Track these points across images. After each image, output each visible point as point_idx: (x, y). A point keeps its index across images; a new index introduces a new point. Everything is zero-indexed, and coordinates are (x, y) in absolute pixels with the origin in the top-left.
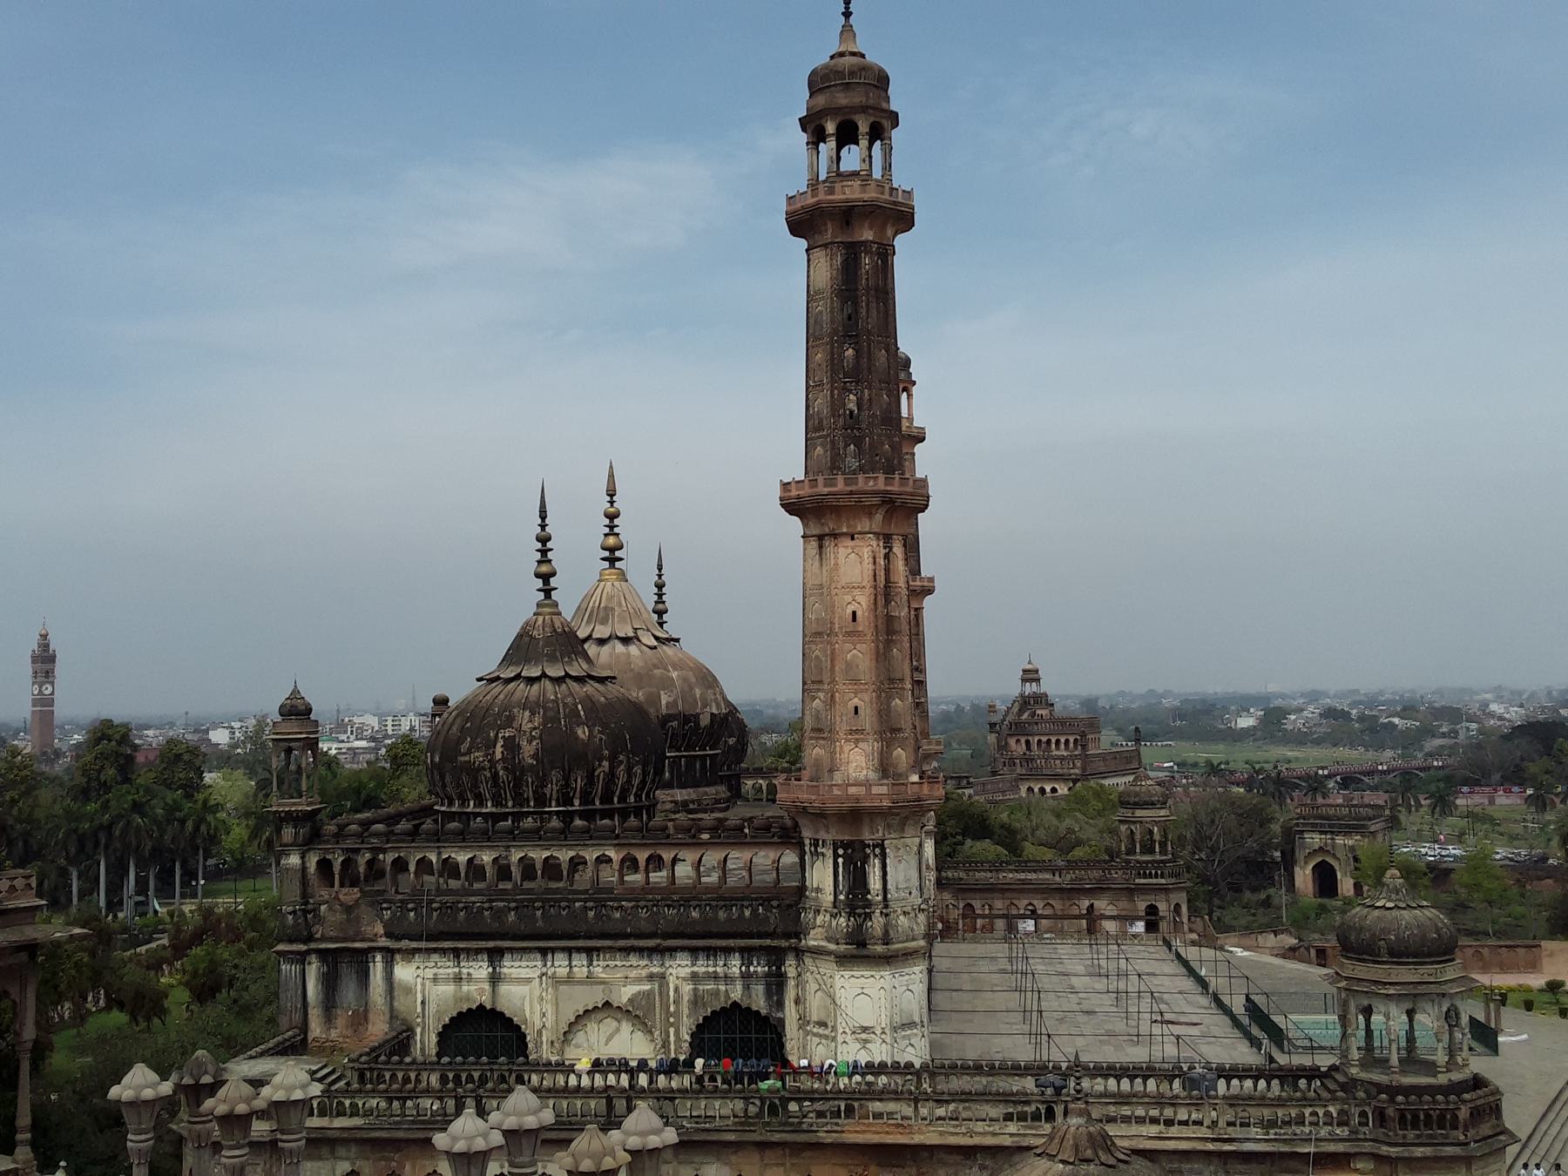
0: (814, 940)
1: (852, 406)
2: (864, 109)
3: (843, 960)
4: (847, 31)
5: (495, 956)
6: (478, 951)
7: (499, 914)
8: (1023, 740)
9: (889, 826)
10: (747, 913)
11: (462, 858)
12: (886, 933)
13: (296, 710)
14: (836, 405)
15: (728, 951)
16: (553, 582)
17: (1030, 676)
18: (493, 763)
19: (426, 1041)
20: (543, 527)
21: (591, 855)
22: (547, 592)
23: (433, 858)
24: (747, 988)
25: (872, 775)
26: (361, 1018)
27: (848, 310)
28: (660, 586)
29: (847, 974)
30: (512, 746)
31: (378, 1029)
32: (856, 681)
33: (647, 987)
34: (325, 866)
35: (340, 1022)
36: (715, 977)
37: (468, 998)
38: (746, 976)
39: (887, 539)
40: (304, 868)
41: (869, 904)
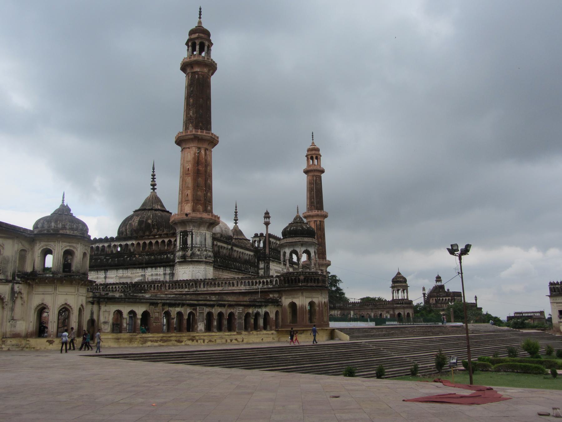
0: (177, 260)
1: (191, 114)
2: (197, 38)
4: (200, 22)
5: (106, 270)
6: (102, 270)
7: (108, 260)
8: (434, 299)
9: (194, 226)
10: (165, 256)
11: (101, 245)
12: (191, 255)
15: (160, 267)
16: (155, 187)
17: (438, 279)
18: (126, 230)
20: (153, 172)
21: (129, 243)
22: (154, 189)
23: (94, 246)
24: (165, 277)
27: (192, 89)
28: (236, 212)
29: (181, 267)
32: (188, 187)
33: (141, 278)
36: (157, 275)
38: (165, 274)
39: (199, 148)
41: (187, 248)
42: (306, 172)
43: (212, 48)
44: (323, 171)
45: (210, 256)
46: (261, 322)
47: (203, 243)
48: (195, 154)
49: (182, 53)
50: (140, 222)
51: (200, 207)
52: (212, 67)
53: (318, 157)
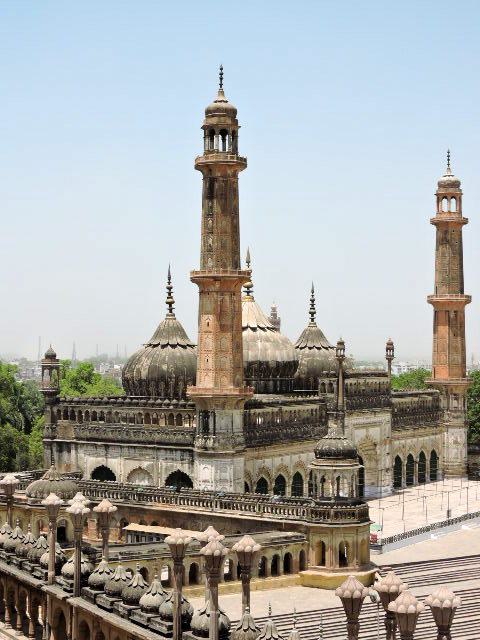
1: (210, 241)
3: (201, 455)
13: (51, 357)
14: (205, 242)
15: (176, 450)
19: (87, 476)
20: (169, 283)
25: (211, 385)
26: (68, 467)
28: (313, 301)
30: (139, 372)
31: (74, 470)
34: (59, 411)
35: (63, 468)
37: (98, 462)
40: (52, 412)
42: (434, 222)
43: (240, 131)
44: (465, 221)
45: (240, 444)
46: (281, 565)
47: (230, 427)
48: (216, 302)
49: (197, 146)
50: (152, 369)
51: (226, 380)
52: (242, 163)
53: (458, 197)
